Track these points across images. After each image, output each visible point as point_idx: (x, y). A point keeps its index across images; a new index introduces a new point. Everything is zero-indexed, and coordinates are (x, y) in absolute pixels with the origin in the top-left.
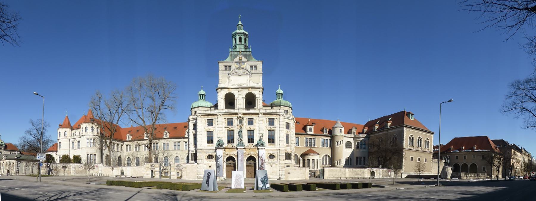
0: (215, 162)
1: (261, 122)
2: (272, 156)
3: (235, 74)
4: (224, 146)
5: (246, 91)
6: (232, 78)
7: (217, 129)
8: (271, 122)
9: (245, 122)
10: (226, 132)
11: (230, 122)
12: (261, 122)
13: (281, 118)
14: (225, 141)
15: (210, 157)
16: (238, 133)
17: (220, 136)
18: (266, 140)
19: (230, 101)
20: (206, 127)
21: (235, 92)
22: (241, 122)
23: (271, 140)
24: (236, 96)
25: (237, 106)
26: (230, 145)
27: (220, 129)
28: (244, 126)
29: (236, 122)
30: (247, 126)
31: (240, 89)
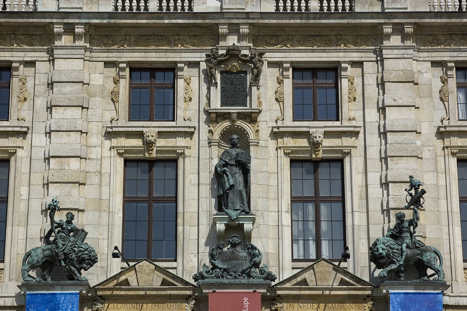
1: (396, 94)
4: (93, 276)
7: (38, 139)
11: (151, 91)
12: (396, 94)
14: (104, 230)
27: (64, 143)
28: (266, 123)
29: (194, 95)
30: (289, 122)
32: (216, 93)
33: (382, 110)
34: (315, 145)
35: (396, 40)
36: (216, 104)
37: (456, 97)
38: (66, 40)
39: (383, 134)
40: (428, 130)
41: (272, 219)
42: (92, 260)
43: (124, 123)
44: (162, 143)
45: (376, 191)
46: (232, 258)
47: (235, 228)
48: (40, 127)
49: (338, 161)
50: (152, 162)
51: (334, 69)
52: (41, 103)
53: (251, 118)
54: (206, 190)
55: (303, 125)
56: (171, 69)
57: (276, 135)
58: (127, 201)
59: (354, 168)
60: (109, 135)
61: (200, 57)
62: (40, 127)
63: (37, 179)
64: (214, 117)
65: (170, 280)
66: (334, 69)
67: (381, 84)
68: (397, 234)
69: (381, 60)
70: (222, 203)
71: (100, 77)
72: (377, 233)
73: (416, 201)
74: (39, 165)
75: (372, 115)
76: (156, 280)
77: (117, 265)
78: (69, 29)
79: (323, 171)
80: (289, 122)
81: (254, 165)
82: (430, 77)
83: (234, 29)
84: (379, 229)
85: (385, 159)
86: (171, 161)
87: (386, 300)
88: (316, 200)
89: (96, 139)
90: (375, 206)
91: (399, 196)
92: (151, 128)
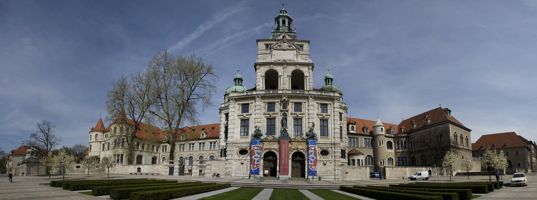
0: (249, 158)
1: (311, 108)
2: (325, 153)
3: (279, 48)
4: (262, 138)
5: (291, 69)
6: (274, 52)
7: (253, 115)
8: (324, 107)
9: (291, 107)
10: (265, 120)
11: (271, 107)
13: (337, 104)
14: (264, 131)
15: (243, 152)
16: (282, 121)
17: (258, 125)
18: (317, 131)
19: (272, 80)
20: (240, 113)
21: (279, 69)
22: (285, 107)
23: (324, 132)
24: (280, 73)
25: (281, 86)
26: (270, 138)
27: (257, 116)
28: (290, 112)
29: (278, 107)
30: (293, 112)
31: (285, 66)
32: (282, 107)
33: (308, 110)
34: (298, 116)
35: (311, 99)
36: (282, 109)
37: (320, 109)
38: (258, 99)
39: (308, 114)
40: (315, 114)
41: (290, 128)
42: (262, 135)
43: (267, 112)
44: (273, 115)
45: (307, 124)
46: (284, 135)
47: (285, 130)
48: (254, 114)
49: (301, 119)
50: (271, 119)
51: (301, 103)
52: (254, 109)
53: (287, 111)
54: (280, 123)
55: (296, 112)
56: (274, 103)
57: (291, 114)
58: (267, 125)
59: (304, 120)
60: (264, 114)
61: (279, 101)
62: (254, 114)
63: (253, 122)
64: (281, 111)
65: (274, 138)
66: (301, 103)
67: (308, 106)
68: (310, 131)
69: (308, 102)
70: (282, 126)
71: (263, 105)
72: (307, 131)
73: (313, 126)
74: (254, 120)
75: (307, 111)
76: (272, 138)
77: (266, 136)
78: (258, 97)
79: (299, 120)
80: (293, 112)
81: (288, 119)
82: (316, 105)
83: (285, 96)
84: (308, 130)
85: (309, 119)
86: (274, 118)
87: (308, 142)
88: (298, 125)
89: (262, 115)
90: (307, 127)
91: (311, 125)
92: (271, 113)
